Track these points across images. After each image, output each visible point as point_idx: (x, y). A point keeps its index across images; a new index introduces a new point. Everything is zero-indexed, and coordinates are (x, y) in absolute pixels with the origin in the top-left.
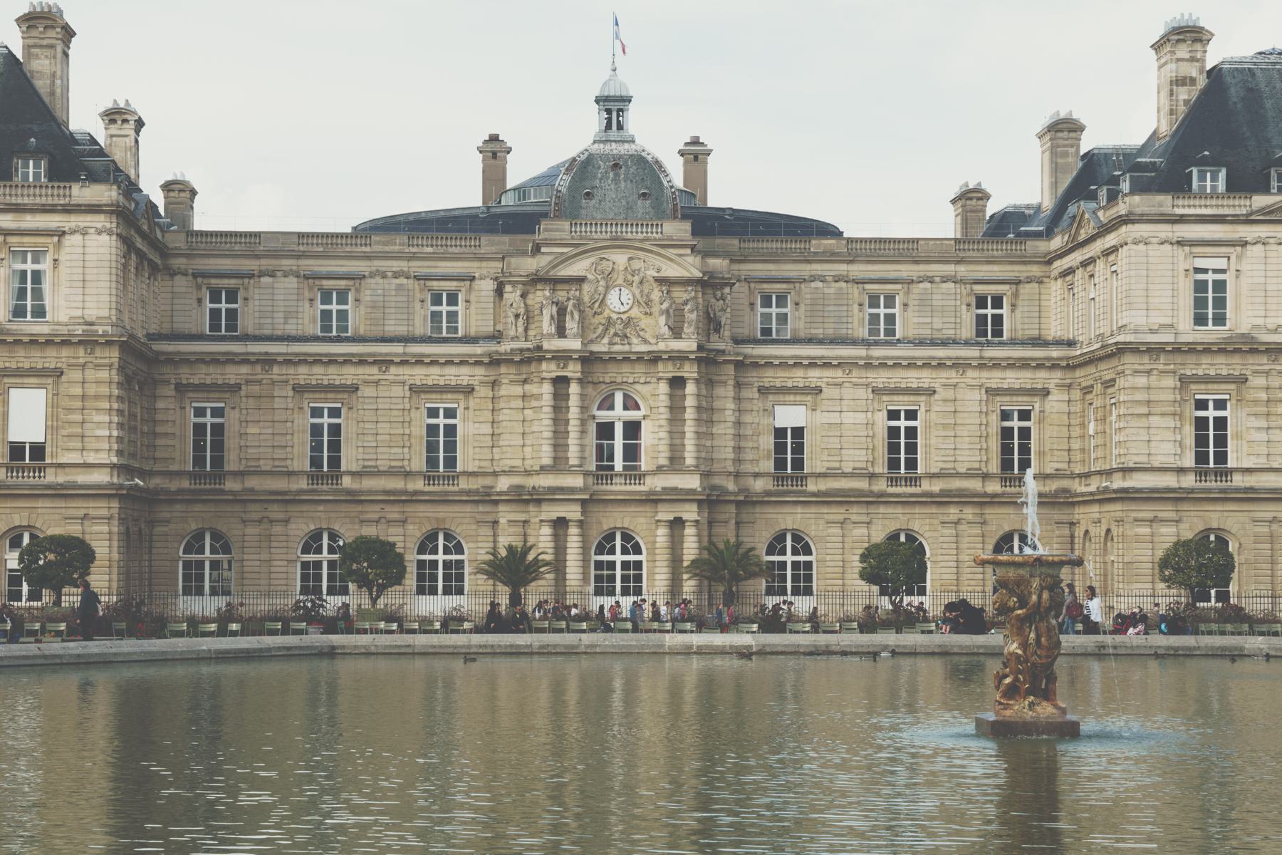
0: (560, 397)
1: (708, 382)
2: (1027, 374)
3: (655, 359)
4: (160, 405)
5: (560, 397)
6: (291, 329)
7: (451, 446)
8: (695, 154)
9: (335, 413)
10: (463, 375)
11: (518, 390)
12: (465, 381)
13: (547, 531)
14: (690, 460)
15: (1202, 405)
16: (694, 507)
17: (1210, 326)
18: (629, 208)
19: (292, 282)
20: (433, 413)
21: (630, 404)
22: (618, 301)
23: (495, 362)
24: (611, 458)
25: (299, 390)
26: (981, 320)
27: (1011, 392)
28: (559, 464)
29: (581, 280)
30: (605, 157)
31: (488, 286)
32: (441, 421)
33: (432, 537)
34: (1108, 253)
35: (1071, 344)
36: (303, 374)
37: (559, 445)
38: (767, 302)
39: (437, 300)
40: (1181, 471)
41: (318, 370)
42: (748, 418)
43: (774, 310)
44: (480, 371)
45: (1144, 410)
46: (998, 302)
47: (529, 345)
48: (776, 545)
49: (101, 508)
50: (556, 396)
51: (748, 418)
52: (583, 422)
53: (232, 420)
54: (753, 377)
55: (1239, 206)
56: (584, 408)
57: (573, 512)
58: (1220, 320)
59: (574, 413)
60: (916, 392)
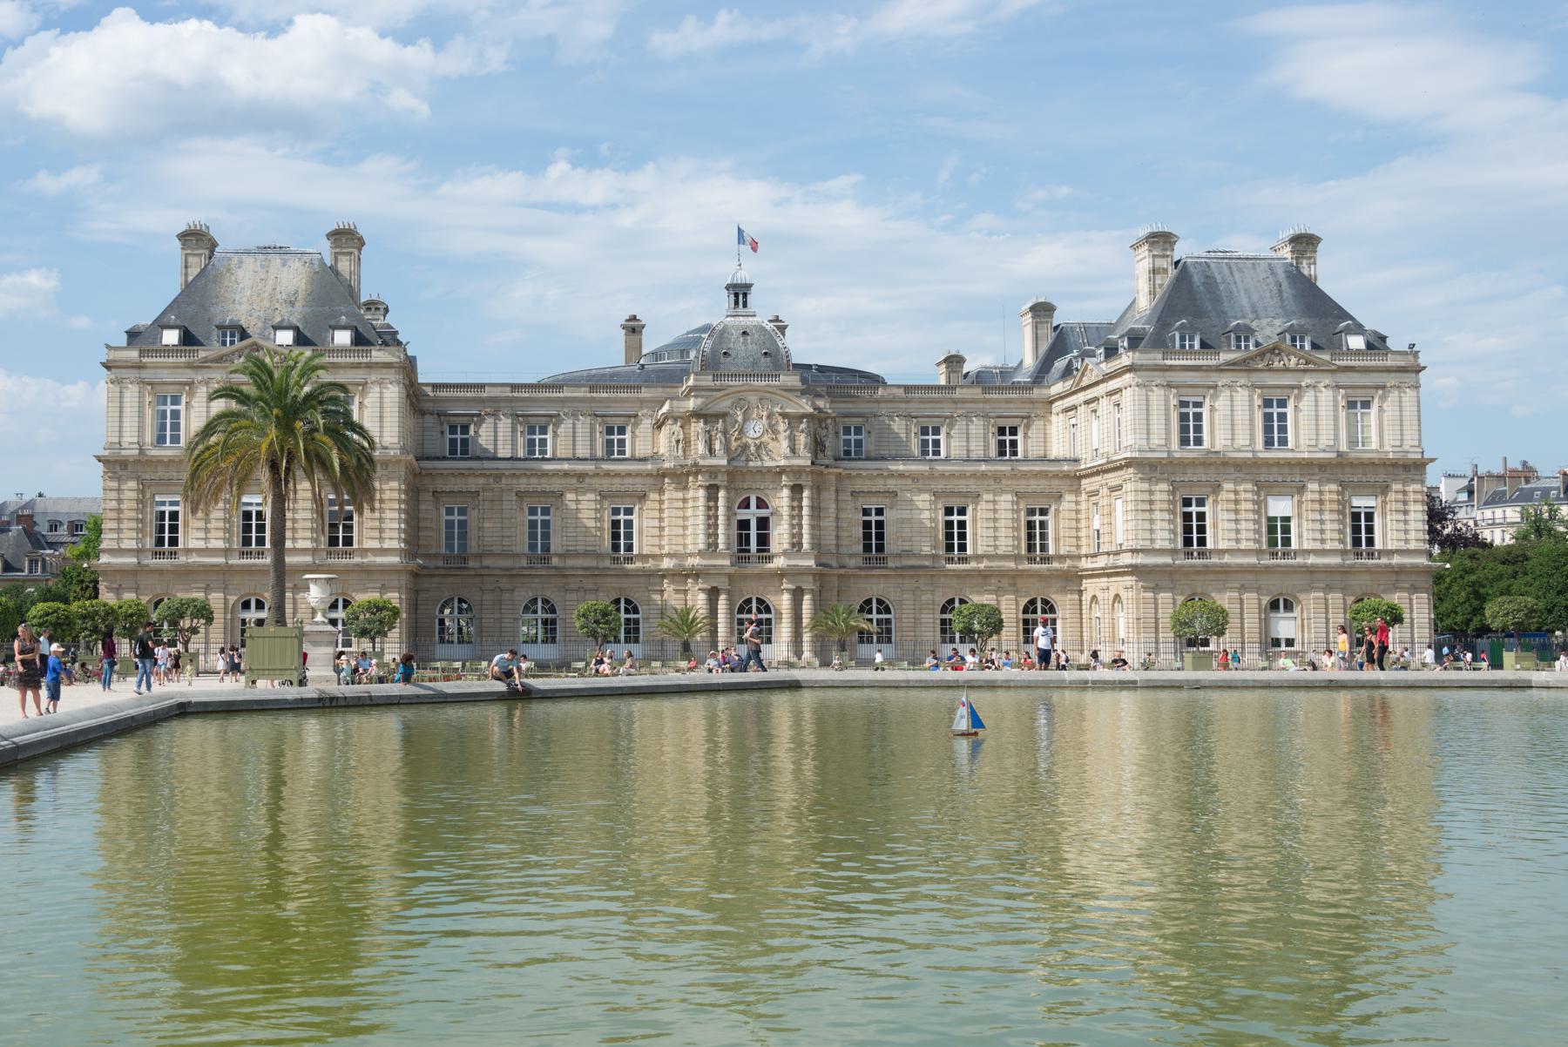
1: (818, 490)
2: (1045, 482)
3: (782, 471)
9: (546, 511)
10: (638, 485)
11: (680, 495)
12: (639, 488)
13: (702, 597)
14: (806, 546)
15: (1187, 502)
16: (811, 578)
17: (1192, 447)
18: (755, 363)
22: (755, 430)
23: (663, 475)
24: (748, 543)
26: (1002, 444)
27: (1034, 494)
28: (712, 545)
29: (724, 416)
30: (737, 328)
31: (647, 424)
32: (622, 517)
33: (617, 601)
34: (1110, 394)
35: (1076, 461)
37: (712, 535)
38: (847, 431)
39: (610, 431)
40: (1173, 552)
42: (843, 515)
43: (853, 437)
44: (650, 481)
45: (1147, 507)
46: (1014, 431)
47: (690, 462)
48: (866, 607)
50: (709, 499)
52: (728, 518)
54: (849, 486)
55: (1211, 361)
56: (729, 508)
57: (723, 583)
58: (1199, 441)
59: (721, 511)
60: (965, 495)
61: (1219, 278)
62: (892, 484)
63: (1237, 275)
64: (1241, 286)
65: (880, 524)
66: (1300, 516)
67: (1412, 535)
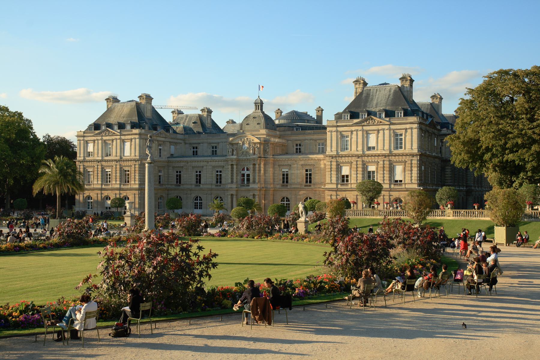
0: (232, 168)
4: (170, 171)
5: (232, 168)
6: (206, 154)
7: (221, 179)
8: (320, 110)
10: (222, 164)
12: (222, 165)
13: (229, 196)
19: (206, 145)
20: (217, 172)
21: (248, 170)
25: (193, 167)
28: (232, 182)
32: (219, 173)
36: (194, 164)
37: (232, 179)
41: (196, 163)
42: (276, 172)
44: (225, 163)
49: (137, 192)
51: (276, 172)
53: (182, 174)
57: (234, 193)
61: (371, 94)
62: (289, 162)
63: (378, 93)
64: (377, 96)
65: (287, 175)
66: (377, 172)
67: (413, 178)
